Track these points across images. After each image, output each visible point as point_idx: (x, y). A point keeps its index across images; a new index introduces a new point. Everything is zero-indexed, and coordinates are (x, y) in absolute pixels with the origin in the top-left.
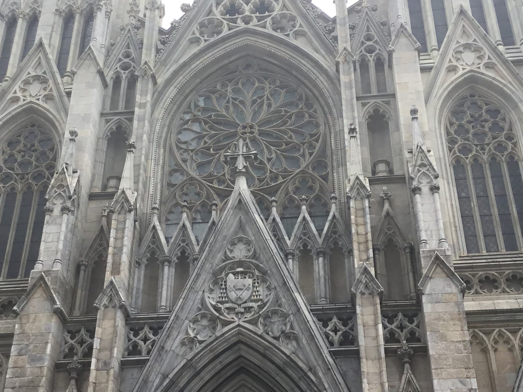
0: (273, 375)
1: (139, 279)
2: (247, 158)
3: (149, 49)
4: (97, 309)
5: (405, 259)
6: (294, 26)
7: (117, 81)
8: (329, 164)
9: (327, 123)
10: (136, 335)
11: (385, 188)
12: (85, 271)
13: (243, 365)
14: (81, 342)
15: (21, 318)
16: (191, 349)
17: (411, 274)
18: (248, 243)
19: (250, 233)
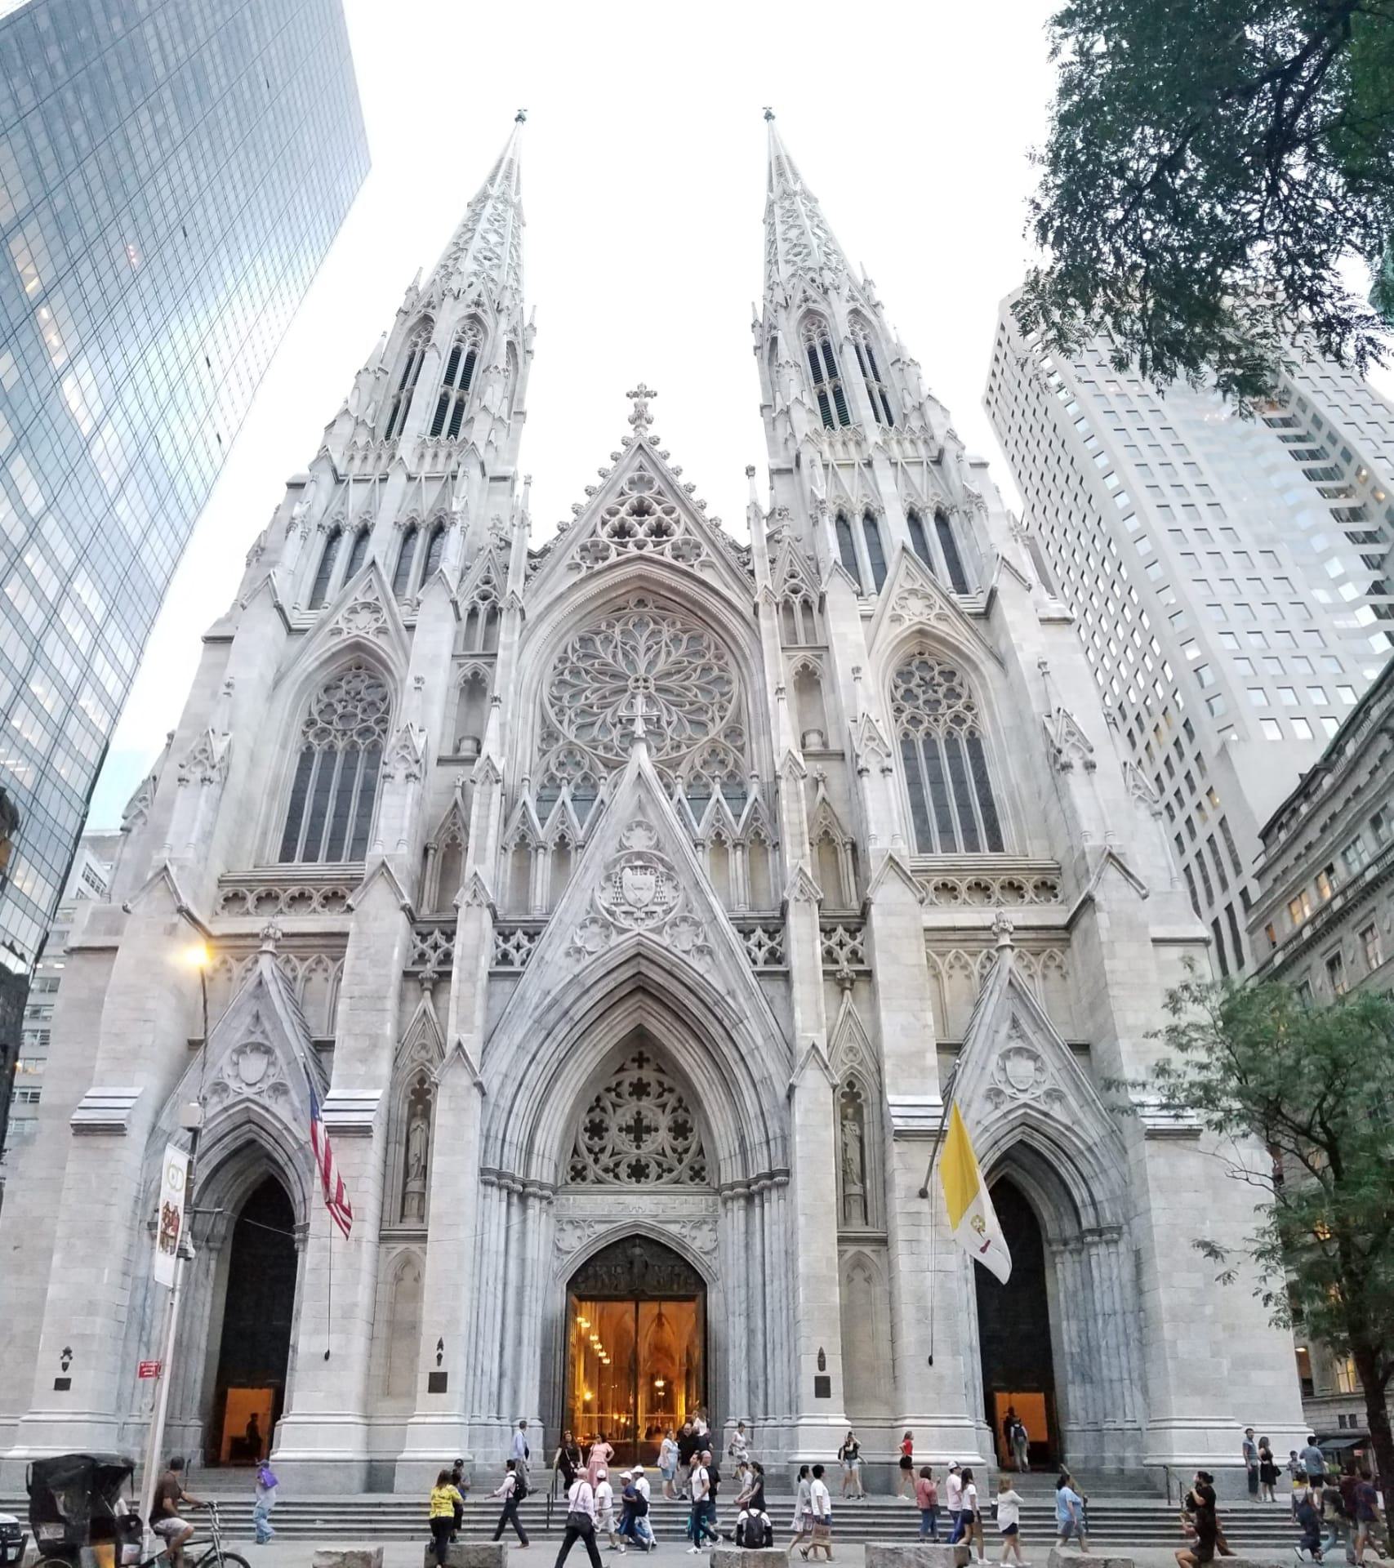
0: (681, 997)
1: (505, 871)
2: (647, 720)
3: (516, 575)
4: (457, 908)
5: (845, 858)
6: (699, 555)
7: (473, 614)
8: (746, 731)
9: (742, 679)
10: (506, 939)
11: (819, 766)
14: (435, 947)
17: (852, 878)
18: (649, 828)
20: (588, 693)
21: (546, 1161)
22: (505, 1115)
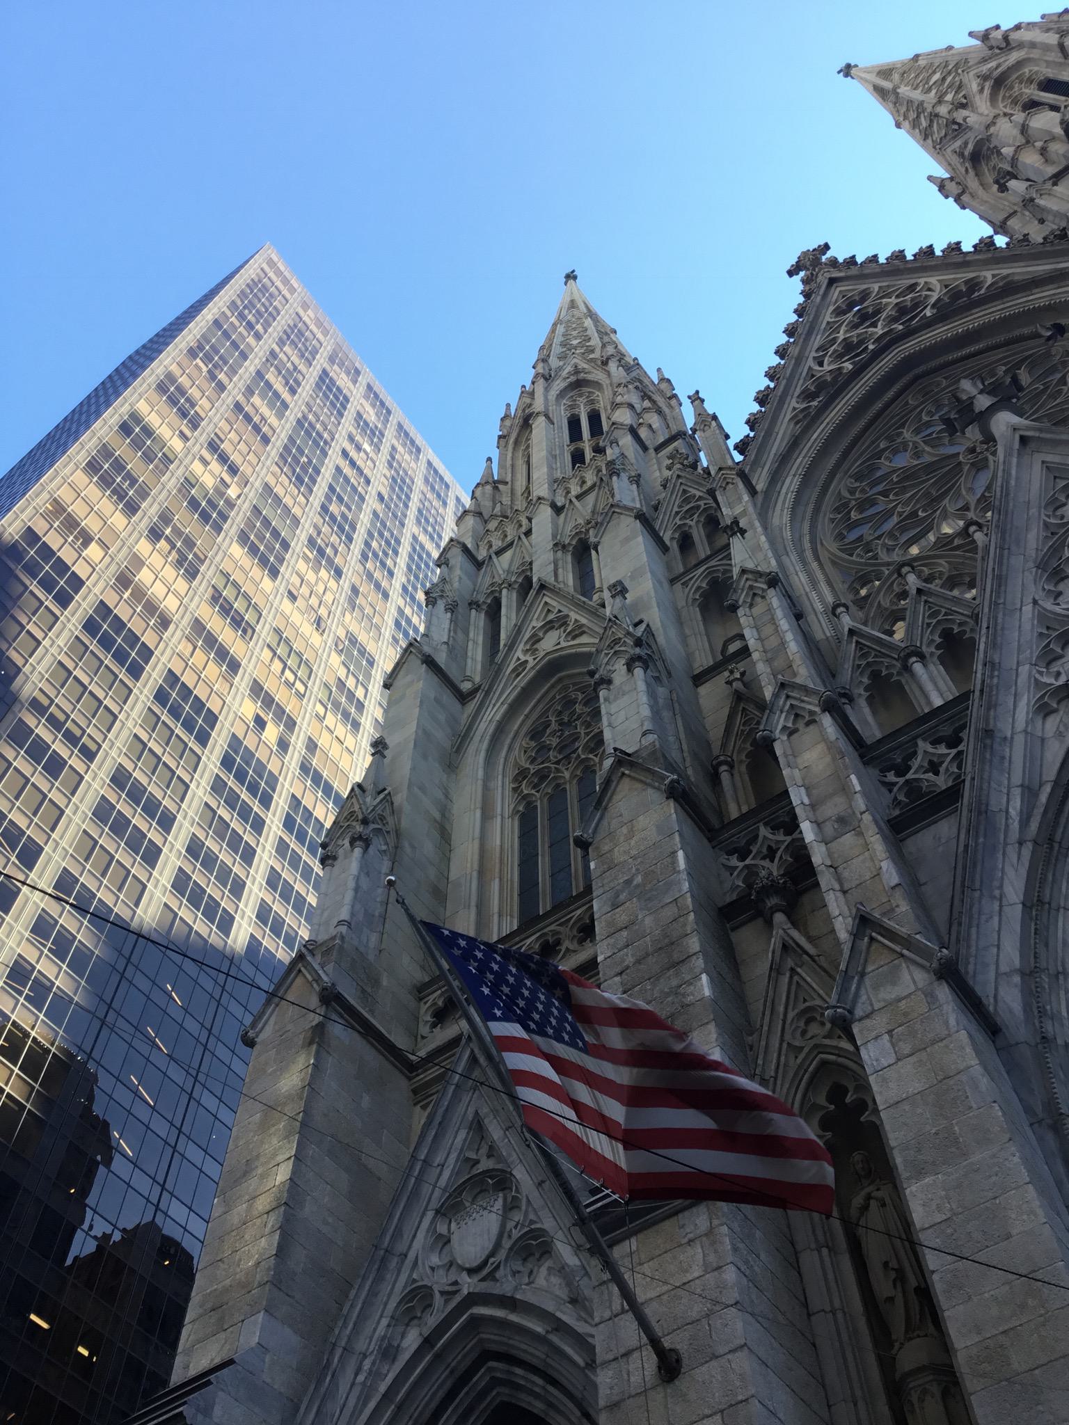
10: (902, 770)
12: (732, 775)
15: (597, 848)
20: (899, 509)
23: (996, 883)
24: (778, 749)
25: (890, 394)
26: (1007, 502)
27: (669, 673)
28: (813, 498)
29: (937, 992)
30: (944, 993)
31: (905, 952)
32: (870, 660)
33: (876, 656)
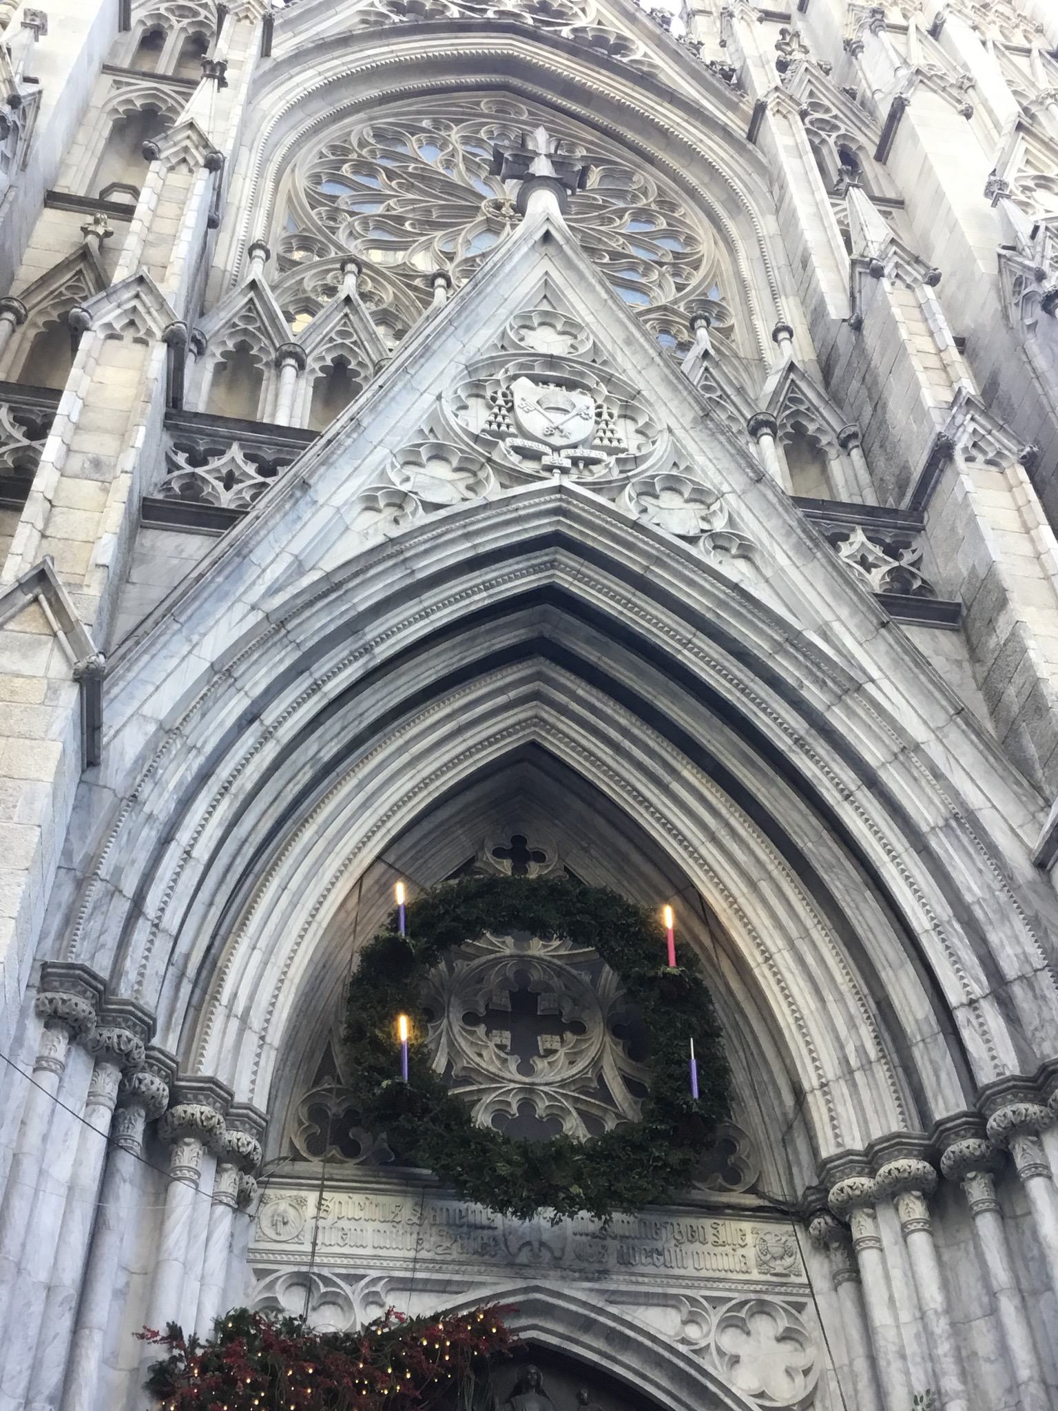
0: (669, 645)
12: (13, 331)
13: (547, 630)
16: (396, 521)
19: (580, 307)
20: (392, 202)
21: (251, 1040)
22: (149, 836)
23: (202, 629)
24: (86, 340)
25: (471, 79)
26: (488, 284)
27: (24, 166)
28: (322, 114)
29: (63, 692)
30: (70, 696)
31: (61, 634)
32: (250, 328)
33: (259, 329)
